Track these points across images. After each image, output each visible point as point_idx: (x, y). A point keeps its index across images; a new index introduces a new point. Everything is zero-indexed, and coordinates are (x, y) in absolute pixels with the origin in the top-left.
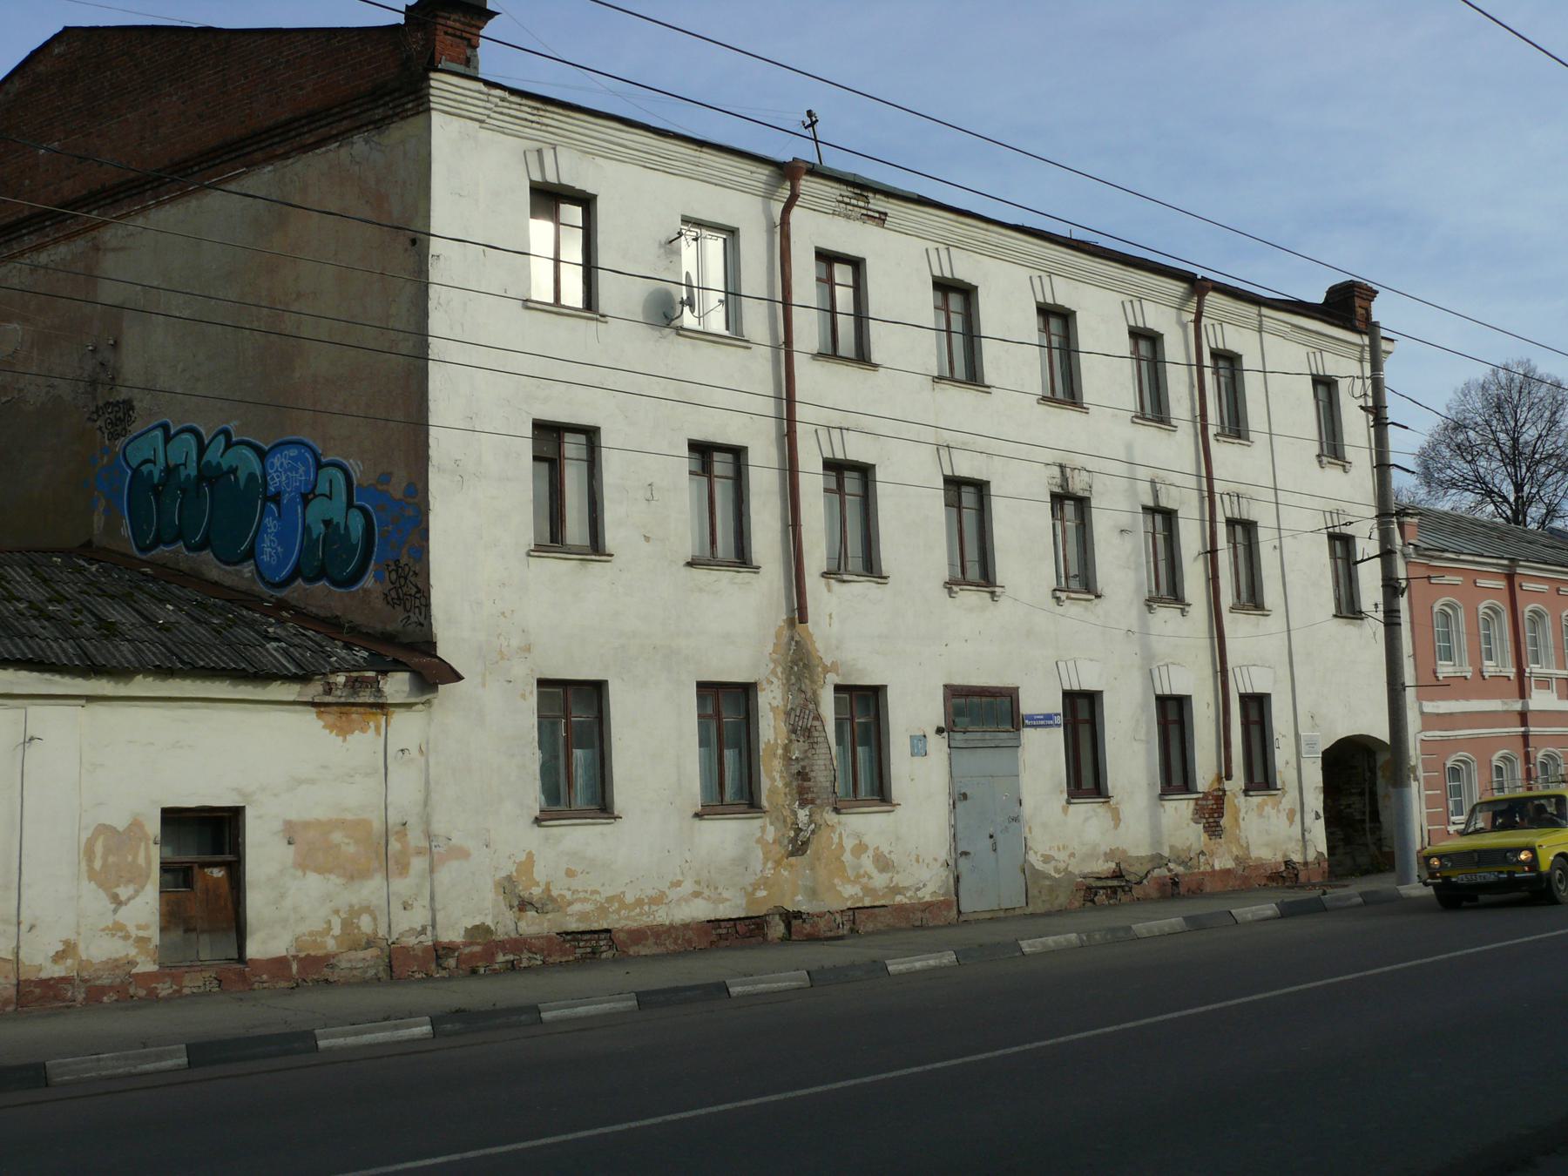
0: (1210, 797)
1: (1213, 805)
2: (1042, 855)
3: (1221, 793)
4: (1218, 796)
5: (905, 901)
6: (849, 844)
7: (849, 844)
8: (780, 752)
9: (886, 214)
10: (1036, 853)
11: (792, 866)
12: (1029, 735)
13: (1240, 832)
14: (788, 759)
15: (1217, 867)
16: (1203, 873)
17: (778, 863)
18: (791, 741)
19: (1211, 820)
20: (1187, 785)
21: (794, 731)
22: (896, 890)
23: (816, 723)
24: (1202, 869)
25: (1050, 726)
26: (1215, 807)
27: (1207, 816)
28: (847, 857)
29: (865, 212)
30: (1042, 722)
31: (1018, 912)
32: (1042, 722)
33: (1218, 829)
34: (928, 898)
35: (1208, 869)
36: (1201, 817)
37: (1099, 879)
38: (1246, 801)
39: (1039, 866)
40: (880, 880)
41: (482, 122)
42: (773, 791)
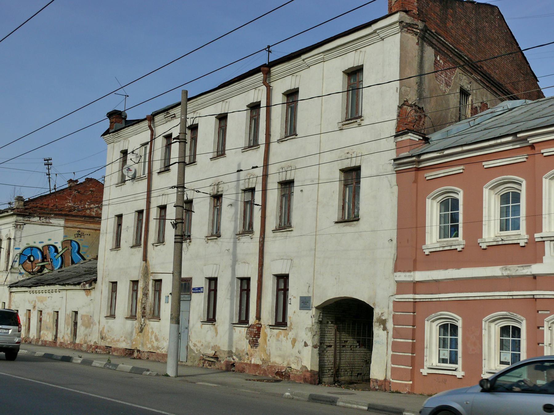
0: (255, 327)
1: (256, 331)
2: (194, 343)
3: (260, 326)
4: (259, 327)
5: (159, 352)
6: (150, 330)
7: (150, 330)
8: (141, 301)
9: (174, 114)
10: (192, 342)
11: (140, 335)
12: (195, 297)
13: (267, 346)
14: (142, 303)
15: (253, 362)
16: (246, 364)
17: (138, 334)
18: (143, 297)
19: (254, 339)
20: (246, 321)
21: (144, 295)
22: (158, 348)
23: (148, 292)
24: (246, 362)
25: (199, 292)
26: (257, 332)
27: (253, 336)
28: (150, 335)
29: (171, 117)
30: (197, 291)
31: (183, 363)
32: (197, 291)
33: (257, 343)
34: (163, 353)
35: (249, 362)
36: (250, 337)
37: (209, 357)
38: (271, 331)
39: (192, 347)
40: (155, 344)
41: (113, 142)
42: (139, 313)
